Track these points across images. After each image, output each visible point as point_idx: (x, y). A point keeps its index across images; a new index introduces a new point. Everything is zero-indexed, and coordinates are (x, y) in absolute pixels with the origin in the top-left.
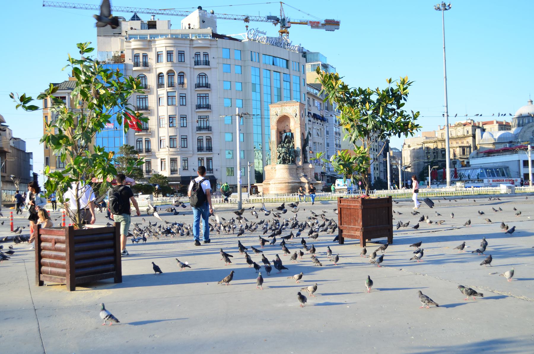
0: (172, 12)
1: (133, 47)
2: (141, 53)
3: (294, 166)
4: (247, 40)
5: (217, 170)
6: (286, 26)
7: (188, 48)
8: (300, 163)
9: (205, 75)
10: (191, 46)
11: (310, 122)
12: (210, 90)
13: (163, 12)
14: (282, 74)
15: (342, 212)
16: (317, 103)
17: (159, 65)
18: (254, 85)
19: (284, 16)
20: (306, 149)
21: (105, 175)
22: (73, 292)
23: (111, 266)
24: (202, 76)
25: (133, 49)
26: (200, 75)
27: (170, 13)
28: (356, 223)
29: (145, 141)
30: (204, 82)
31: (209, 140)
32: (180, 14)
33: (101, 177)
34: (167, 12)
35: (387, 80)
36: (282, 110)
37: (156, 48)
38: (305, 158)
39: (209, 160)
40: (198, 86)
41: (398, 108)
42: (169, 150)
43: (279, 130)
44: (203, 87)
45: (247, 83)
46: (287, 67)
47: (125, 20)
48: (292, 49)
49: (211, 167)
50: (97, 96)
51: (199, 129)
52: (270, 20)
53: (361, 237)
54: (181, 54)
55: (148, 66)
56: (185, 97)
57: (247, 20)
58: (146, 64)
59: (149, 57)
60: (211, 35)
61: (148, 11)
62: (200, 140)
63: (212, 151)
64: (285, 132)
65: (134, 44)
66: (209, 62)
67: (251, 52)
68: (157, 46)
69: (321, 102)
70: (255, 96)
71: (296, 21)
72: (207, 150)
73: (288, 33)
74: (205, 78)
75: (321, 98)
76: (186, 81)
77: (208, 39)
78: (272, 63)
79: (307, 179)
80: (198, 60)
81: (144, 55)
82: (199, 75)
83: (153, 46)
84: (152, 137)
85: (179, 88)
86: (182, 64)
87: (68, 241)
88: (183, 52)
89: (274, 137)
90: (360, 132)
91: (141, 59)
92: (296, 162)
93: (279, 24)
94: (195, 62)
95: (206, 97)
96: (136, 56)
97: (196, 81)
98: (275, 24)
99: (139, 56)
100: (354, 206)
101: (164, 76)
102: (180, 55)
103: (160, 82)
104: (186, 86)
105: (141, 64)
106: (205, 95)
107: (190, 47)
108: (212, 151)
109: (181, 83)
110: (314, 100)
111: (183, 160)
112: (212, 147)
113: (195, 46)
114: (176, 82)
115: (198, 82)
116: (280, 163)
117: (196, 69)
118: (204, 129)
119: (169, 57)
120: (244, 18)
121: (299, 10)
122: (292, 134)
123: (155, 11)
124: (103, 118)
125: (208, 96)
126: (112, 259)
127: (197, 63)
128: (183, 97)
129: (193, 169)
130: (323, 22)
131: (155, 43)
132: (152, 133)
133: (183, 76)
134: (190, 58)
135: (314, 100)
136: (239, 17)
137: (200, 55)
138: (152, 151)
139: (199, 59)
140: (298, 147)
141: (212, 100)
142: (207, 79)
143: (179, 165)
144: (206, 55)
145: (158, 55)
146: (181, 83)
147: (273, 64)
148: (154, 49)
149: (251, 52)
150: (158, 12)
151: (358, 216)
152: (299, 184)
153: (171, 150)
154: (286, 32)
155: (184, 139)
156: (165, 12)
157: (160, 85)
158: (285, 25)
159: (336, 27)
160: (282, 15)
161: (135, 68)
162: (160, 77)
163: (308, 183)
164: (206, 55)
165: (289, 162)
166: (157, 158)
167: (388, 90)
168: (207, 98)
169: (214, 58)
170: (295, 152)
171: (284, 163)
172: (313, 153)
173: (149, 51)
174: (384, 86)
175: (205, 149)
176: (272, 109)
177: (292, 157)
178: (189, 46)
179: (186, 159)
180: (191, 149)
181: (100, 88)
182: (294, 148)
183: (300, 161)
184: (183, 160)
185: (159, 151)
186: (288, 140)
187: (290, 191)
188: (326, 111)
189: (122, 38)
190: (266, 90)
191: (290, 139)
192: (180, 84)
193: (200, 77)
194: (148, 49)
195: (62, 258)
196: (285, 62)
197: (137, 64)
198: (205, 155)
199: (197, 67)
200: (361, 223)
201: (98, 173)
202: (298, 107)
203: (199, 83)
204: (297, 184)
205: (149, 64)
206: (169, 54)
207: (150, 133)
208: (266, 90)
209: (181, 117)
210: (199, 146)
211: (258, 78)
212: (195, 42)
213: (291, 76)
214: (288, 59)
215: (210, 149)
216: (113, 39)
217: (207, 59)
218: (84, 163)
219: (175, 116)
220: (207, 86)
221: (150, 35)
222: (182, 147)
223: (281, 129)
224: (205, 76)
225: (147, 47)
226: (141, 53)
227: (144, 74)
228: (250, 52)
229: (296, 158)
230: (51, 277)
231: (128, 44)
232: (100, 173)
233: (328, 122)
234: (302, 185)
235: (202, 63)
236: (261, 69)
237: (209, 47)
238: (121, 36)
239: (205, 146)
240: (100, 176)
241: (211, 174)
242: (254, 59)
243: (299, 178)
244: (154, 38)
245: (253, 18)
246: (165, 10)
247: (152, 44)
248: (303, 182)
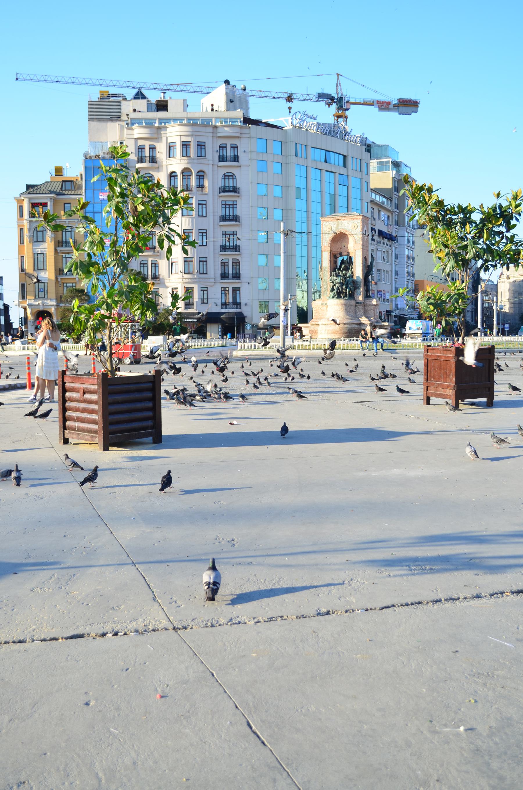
0: (188, 88)
1: (136, 137)
2: (147, 144)
3: (352, 302)
4: (291, 127)
5: (246, 305)
6: (344, 107)
7: (211, 138)
8: (361, 298)
9: (233, 175)
10: (215, 135)
11: (373, 242)
12: (239, 196)
13: (175, 87)
14: (337, 175)
15: (429, 365)
16: (384, 215)
17: (171, 161)
18: (299, 189)
19: (342, 93)
20: (369, 279)
21: (144, 311)
22: (106, 452)
23: (150, 423)
24: (229, 176)
25: (137, 139)
26: (226, 174)
27: (185, 89)
28: (447, 379)
29: (152, 264)
30: (231, 185)
31: (237, 263)
32: (198, 90)
33: (138, 313)
34: (182, 87)
35: (494, 194)
36: (338, 225)
37: (167, 137)
38: (367, 290)
39: (236, 290)
40: (223, 190)
41: (508, 231)
42: (183, 277)
43: (334, 253)
44: (229, 191)
45: (290, 187)
46: (345, 166)
47: (126, 99)
48: (352, 139)
49: (238, 301)
50: (136, 213)
51: (224, 248)
52: (321, 99)
53: (453, 397)
54: (201, 146)
55: (156, 163)
56: (205, 204)
57: (290, 99)
58: (153, 160)
59: (158, 149)
60: (242, 119)
61: (155, 86)
62: (224, 264)
63: (240, 279)
64: (341, 255)
65: (138, 132)
66: (238, 157)
67: (296, 143)
68: (168, 135)
69: (390, 215)
70: (299, 205)
71: (358, 101)
72: (233, 277)
73: (346, 117)
74: (233, 179)
75: (390, 208)
76: (206, 183)
77: (238, 126)
78: (323, 160)
79: (370, 320)
80: (223, 155)
81: (151, 147)
82: (225, 175)
83: (163, 135)
84: (160, 259)
85: (198, 193)
86: (202, 160)
87: (101, 391)
88: (203, 144)
89: (326, 262)
90: (456, 261)
91: (147, 153)
92: (355, 296)
93: (334, 105)
95: (233, 205)
96: (141, 149)
97: (220, 183)
98: (329, 105)
99: (144, 148)
100: (446, 357)
101: (177, 176)
102: (200, 147)
103: (172, 184)
104: (206, 190)
106: (231, 203)
107: (213, 137)
108: (240, 279)
109: (199, 185)
110: (379, 211)
111: (201, 290)
112: (240, 274)
113: (219, 135)
114: (194, 185)
115: (223, 185)
116: (333, 297)
117: (220, 166)
118: (230, 248)
119: (184, 150)
120: (286, 96)
121: (363, 86)
122: (350, 258)
123: (165, 86)
124: (142, 240)
125: (236, 204)
126: (150, 414)
127: (222, 159)
128: (202, 204)
129: (215, 303)
130: (396, 102)
131: (166, 130)
132: (160, 254)
133: (203, 176)
134: (213, 151)
135: (379, 211)
136: (280, 95)
137: (226, 147)
138: (161, 277)
139: (225, 153)
140: (358, 277)
141: (242, 210)
142: (234, 180)
143: (196, 297)
144: (234, 147)
145: (170, 147)
146: (199, 185)
147: (326, 161)
148: (164, 139)
149: (296, 143)
150: (169, 87)
151: (450, 370)
152: (359, 326)
153: (186, 276)
154: (344, 116)
155: (203, 262)
156: (178, 88)
158: (342, 107)
159: (414, 109)
160: (339, 91)
161: (138, 165)
162: (172, 178)
163: (371, 325)
164: (234, 147)
165: (346, 296)
166: (167, 287)
167: (496, 207)
168: (234, 206)
169: (245, 152)
170: (354, 282)
171: (339, 297)
172: (376, 283)
173: (158, 142)
174: (489, 203)
175: (231, 276)
176: (324, 224)
177: (350, 290)
178: (211, 134)
179: (206, 289)
180: (212, 276)
181: (139, 204)
182: (353, 277)
183: (360, 295)
184: (201, 290)
185: (169, 277)
186: (344, 266)
187: (345, 335)
188: (396, 226)
189: (121, 123)
190: (314, 196)
191: (348, 265)
192: (199, 187)
193: (226, 177)
194: (156, 138)
195: (92, 412)
196: (341, 157)
197: (141, 160)
198: (231, 284)
199: (222, 164)
200: (454, 379)
201: (135, 309)
202: (360, 221)
203: (225, 186)
204: (356, 326)
205: (158, 160)
206: (185, 145)
207: (158, 254)
208: (314, 196)
209: (199, 232)
210: (223, 272)
211: (304, 180)
212: (219, 130)
213: (350, 177)
214: (346, 155)
215: (237, 276)
216: (110, 125)
217: (236, 154)
218: (119, 296)
219: (191, 231)
220: (235, 190)
221: (160, 119)
222: (200, 273)
223: (336, 251)
225: (155, 136)
226: (147, 144)
227: (151, 172)
228: (294, 145)
229: (356, 291)
230: (79, 434)
231: (130, 132)
232: (138, 309)
233: (397, 242)
234: (363, 327)
235: (229, 158)
236: (310, 169)
237: (238, 137)
238: (121, 121)
239: (231, 271)
240: (137, 313)
241: (238, 310)
242: (299, 154)
243: (357, 317)
244: (165, 123)
245: (299, 96)
246: (178, 85)
247: (162, 132)
248: (364, 324)
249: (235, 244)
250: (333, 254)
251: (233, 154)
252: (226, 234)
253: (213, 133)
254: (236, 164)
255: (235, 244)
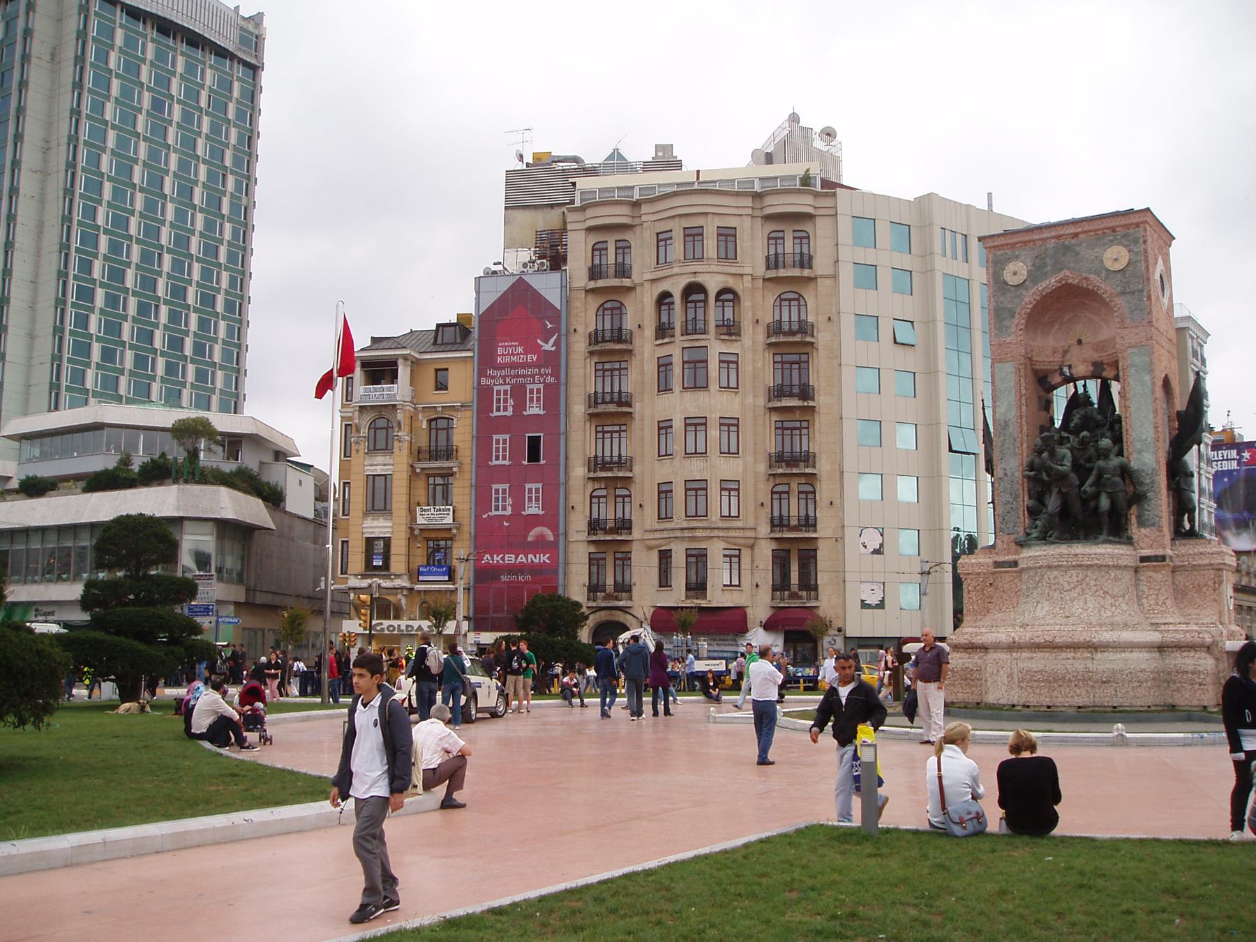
24: (790, 300)
26: (782, 297)
43: (1038, 367)
56: (737, 363)
74: (799, 305)
80: (776, 254)
94: (768, 258)
101: (673, 303)
102: (723, 238)
103: (664, 319)
105: (612, 271)
111: (725, 556)
139: (780, 251)
142: (803, 308)
157: (663, 331)
164: (801, 238)
178: (749, 212)
193: (783, 303)
203: (780, 321)
217: (805, 251)
224: (798, 300)
235: (789, 260)
249: (804, 448)
250: (1035, 372)
251: (798, 250)
252: (783, 429)
253: (752, 208)
254: (806, 273)
255: (804, 448)
